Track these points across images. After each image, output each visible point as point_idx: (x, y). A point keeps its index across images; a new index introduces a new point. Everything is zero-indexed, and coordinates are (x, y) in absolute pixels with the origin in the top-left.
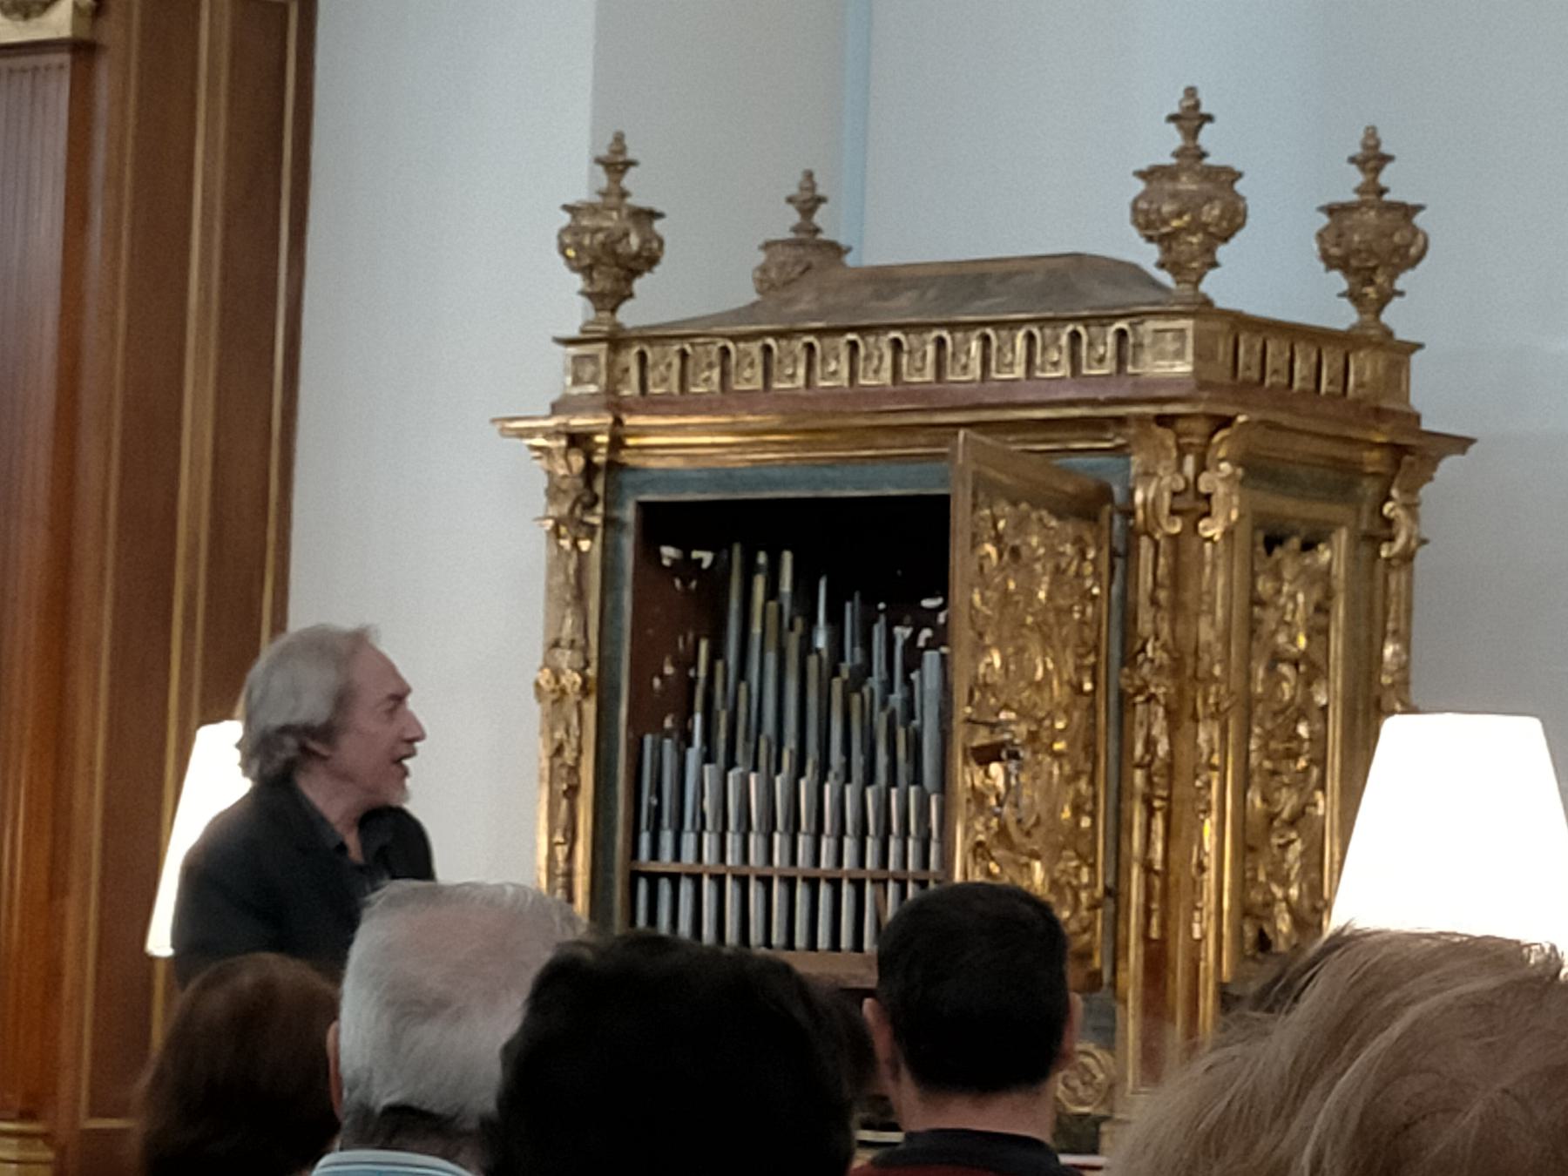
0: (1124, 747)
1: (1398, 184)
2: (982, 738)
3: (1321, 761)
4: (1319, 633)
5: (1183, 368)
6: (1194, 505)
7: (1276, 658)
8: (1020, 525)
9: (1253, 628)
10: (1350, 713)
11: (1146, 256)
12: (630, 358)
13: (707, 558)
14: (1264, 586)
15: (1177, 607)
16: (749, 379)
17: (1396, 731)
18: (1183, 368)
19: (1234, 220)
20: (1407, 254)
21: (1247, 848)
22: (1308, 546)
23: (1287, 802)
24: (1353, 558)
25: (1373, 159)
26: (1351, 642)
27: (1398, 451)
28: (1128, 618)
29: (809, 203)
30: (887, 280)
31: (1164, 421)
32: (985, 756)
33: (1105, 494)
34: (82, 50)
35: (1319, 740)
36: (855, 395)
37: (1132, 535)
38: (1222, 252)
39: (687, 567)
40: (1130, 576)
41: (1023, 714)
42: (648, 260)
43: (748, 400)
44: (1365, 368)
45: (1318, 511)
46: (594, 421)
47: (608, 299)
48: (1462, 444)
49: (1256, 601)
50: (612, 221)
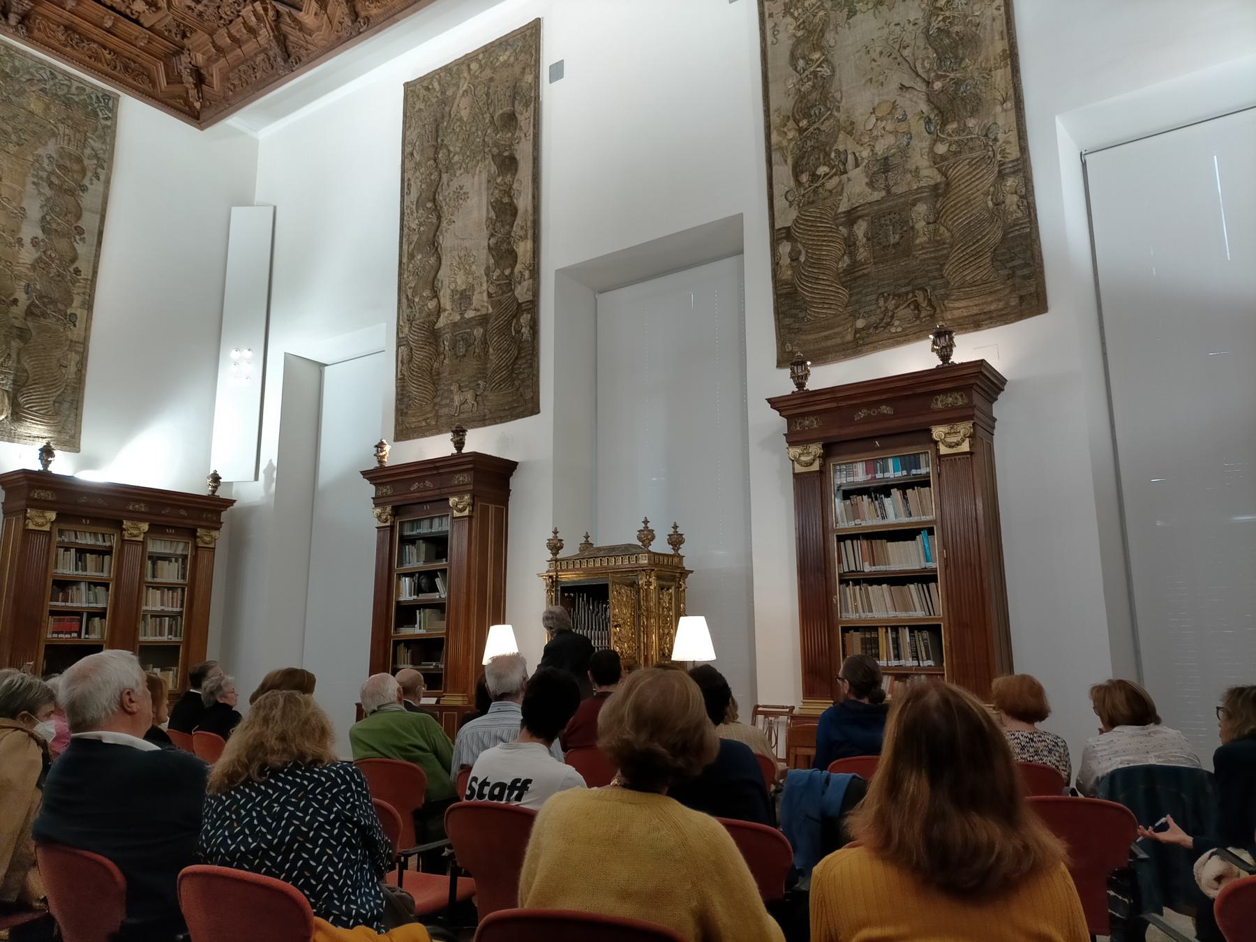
0: (640, 623)
1: (680, 531)
2: (615, 623)
3: (671, 624)
4: (670, 603)
5: (646, 562)
6: (649, 584)
7: (664, 608)
8: (620, 588)
9: (659, 603)
10: (676, 617)
11: (640, 544)
12: (559, 563)
13: (572, 595)
14: (661, 596)
15: (647, 600)
16: (578, 566)
17: (682, 619)
18: (646, 562)
19: (653, 538)
20: (682, 542)
21: (660, 639)
22: (668, 589)
23: (666, 631)
24: (675, 591)
25: (675, 527)
26: (675, 605)
27: (681, 573)
28: (639, 602)
29: (587, 537)
30: (599, 549)
31: (644, 570)
32: (616, 627)
33: (635, 582)
34: (470, 517)
35: (671, 621)
36: (594, 568)
37: (639, 589)
38: (652, 543)
39: (569, 596)
40: (639, 595)
41: (622, 619)
42: (561, 547)
43: (578, 569)
44: (676, 560)
45: (670, 584)
46: (553, 574)
47: (555, 554)
48: (692, 572)
49: (660, 599)
50: (555, 542)
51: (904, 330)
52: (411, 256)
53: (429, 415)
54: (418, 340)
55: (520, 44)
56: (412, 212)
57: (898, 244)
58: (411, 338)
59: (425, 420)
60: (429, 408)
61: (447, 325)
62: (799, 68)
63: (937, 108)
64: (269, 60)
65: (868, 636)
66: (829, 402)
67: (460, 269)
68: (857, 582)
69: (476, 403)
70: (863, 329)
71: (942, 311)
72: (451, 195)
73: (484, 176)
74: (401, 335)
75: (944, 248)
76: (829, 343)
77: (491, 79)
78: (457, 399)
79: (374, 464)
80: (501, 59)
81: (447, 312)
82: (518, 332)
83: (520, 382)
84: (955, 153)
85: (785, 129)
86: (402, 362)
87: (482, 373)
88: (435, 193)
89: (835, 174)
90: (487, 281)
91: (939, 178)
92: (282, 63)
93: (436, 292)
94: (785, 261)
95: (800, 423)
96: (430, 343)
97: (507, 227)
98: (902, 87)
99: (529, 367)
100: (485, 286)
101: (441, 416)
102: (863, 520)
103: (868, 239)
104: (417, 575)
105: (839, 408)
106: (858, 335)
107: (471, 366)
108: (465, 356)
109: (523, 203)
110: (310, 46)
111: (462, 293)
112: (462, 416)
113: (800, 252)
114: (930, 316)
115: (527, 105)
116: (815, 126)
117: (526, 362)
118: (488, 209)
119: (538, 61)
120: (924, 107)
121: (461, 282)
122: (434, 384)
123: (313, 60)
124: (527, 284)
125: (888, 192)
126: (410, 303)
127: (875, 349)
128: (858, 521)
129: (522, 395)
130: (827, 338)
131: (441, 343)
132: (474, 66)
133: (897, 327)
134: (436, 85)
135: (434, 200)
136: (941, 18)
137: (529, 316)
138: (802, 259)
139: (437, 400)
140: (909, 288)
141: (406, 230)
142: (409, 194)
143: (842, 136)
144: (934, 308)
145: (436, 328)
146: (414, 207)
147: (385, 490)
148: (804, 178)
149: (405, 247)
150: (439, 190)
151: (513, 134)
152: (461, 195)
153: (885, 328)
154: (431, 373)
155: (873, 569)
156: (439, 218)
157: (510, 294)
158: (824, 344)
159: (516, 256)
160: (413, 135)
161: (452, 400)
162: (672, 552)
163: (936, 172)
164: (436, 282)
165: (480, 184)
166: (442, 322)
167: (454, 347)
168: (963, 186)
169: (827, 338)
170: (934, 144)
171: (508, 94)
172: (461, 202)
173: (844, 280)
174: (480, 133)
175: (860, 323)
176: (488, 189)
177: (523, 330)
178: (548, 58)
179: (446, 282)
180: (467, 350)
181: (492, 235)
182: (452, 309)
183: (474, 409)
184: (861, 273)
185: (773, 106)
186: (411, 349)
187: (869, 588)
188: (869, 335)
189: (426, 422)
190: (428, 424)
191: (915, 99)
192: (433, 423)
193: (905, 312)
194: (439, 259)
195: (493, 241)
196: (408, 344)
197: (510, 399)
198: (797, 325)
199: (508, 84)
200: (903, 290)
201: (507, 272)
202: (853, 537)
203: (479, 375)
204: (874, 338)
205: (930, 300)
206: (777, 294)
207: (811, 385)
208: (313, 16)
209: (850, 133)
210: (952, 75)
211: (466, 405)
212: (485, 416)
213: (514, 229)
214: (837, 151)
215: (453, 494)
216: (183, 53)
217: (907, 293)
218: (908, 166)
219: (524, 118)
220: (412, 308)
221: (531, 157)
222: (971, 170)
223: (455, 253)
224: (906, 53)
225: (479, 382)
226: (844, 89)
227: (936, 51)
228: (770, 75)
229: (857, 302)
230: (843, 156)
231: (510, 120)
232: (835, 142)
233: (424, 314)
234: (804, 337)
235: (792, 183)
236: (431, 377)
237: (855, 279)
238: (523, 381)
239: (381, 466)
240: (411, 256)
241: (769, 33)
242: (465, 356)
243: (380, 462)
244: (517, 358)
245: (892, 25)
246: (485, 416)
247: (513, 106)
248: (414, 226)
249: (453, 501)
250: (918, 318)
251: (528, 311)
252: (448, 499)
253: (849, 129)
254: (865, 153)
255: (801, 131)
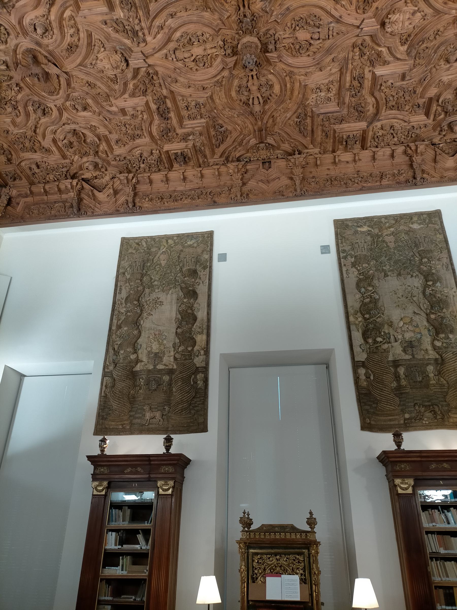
51: (429, 423)
52: (119, 327)
53: (125, 422)
54: (121, 376)
55: (201, 239)
56: (121, 304)
57: (421, 381)
58: (115, 374)
59: (122, 425)
60: (126, 418)
61: (143, 370)
62: (361, 292)
63: (432, 325)
64: (65, 207)
65: (448, 591)
66: (415, 457)
67: (155, 341)
68: (437, 559)
69: (162, 421)
70: (408, 419)
71: (448, 418)
72: (151, 301)
73: (175, 296)
74: (106, 370)
75: (444, 388)
76: (392, 423)
77: (182, 251)
78: (148, 415)
79: (96, 452)
80: (189, 243)
81: (143, 363)
82: (195, 382)
83: (194, 411)
84: (445, 347)
85: (357, 316)
86: (106, 386)
87: (168, 402)
88: (139, 297)
89: (385, 343)
90: (174, 351)
91: (438, 356)
92: (76, 212)
93: (135, 350)
94: (363, 377)
95: (399, 466)
96: (130, 379)
97: (190, 325)
98: (415, 313)
99: (202, 404)
100: (172, 353)
101: (134, 424)
102: (436, 524)
103: (406, 376)
104: (122, 531)
105: (421, 461)
106: (406, 421)
107: (160, 397)
108: (156, 390)
109: (201, 315)
110: (96, 209)
111: (156, 354)
112: (151, 426)
113: (370, 375)
114: (441, 418)
115: (205, 268)
116: (374, 319)
117: (200, 401)
118: (176, 314)
119: (211, 250)
120: (425, 323)
121: (155, 347)
122: (130, 403)
123: (96, 216)
124: (202, 358)
125: (414, 357)
126: (116, 353)
127: (415, 430)
128: (434, 524)
129: (196, 420)
130: (390, 420)
131: (138, 380)
132: (170, 241)
133: (426, 421)
134: (144, 244)
135: (138, 301)
136: (430, 289)
137: (203, 375)
138: (372, 378)
139: (131, 414)
140: (430, 404)
141: (116, 312)
142: (120, 293)
143: (386, 326)
144: (444, 415)
145: (134, 370)
146: (123, 301)
147: (102, 470)
148: (370, 341)
149: (115, 321)
150: (142, 296)
151: (195, 280)
152: (158, 302)
153: (420, 420)
154: (128, 397)
155: (446, 552)
156: (142, 311)
157: (190, 361)
158: (389, 423)
159: (196, 342)
160: (125, 264)
161: (144, 415)
162: (310, 530)
163: (435, 353)
164: (136, 345)
165: (172, 299)
166: (138, 368)
167: (148, 383)
168: (451, 363)
169: (390, 420)
170: (433, 341)
171: (193, 260)
172: (158, 306)
173: (395, 393)
174: (173, 274)
175: (407, 416)
176: (177, 303)
177: (199, 382)
178: (218, 249)
179: (144, 346)
180: (157, 387)
181: (178, 327)
182: (148, 362)
183: (161, 423)
184: (404, 391)
185: (350, 304)
186: (114, 379)
187: (445, 563)
188: (412, 422)
189: (122, 426)
190: (124, 428)
191: (421, 319)
192: (128, 427)
193: (428, 414)
194: (140, 332)
195: (179, 331)
196: (112, 377)
197: (189, 421)
198: (372, 410)
199: (193, 256)
200: (427, 404)
201: (190, 349)
202: (432, 533)
203: (166, 403)
204: (415, 425)
205: (441, 411)
206: (359, 393)
207: (406, 446)
208: (106, 195)
209: (391, 326)
210: (439, 314)
211: (154, 420)
212: (168, 428)
213: (194, 327)
214: (384, 332)
215: (161, 479)
216: (6, 187)
217: (429, 406)
218: (422, 347)
219: (202, 273)
220: (117, 356)
221: (207, 294)
222: (453, 356)
223: (152, 332)
224: (415, 299)
225: (165, 407)
226: (385, 306)
227: (429, 302)
228: (346, 290)
229: (404, 405)
230: (388, 336)
231: (194, 273)
232: (383, 328)
233: (126, 361)
234: (379, 418)
235: (362, 341)
236: (129, 398)
237: (402, 394)
238: (198, 411)
239: (102, 454)
240: (119, 327)
241: (344, 272)
242: (156, 390)
243: (102, 450)
244: (194, 398)
245: (406, 286)
246: (168, 428)
247: (196, 267)
248: (123, 310)
249: (159, 483)
250: (436, 418)
251: (202, 372)
252: (156, 481)
253: (390, 324)
254: (400, 337)
255: (365, 319)
